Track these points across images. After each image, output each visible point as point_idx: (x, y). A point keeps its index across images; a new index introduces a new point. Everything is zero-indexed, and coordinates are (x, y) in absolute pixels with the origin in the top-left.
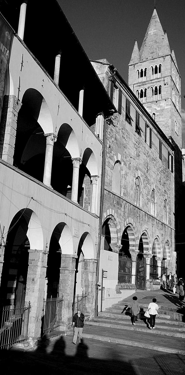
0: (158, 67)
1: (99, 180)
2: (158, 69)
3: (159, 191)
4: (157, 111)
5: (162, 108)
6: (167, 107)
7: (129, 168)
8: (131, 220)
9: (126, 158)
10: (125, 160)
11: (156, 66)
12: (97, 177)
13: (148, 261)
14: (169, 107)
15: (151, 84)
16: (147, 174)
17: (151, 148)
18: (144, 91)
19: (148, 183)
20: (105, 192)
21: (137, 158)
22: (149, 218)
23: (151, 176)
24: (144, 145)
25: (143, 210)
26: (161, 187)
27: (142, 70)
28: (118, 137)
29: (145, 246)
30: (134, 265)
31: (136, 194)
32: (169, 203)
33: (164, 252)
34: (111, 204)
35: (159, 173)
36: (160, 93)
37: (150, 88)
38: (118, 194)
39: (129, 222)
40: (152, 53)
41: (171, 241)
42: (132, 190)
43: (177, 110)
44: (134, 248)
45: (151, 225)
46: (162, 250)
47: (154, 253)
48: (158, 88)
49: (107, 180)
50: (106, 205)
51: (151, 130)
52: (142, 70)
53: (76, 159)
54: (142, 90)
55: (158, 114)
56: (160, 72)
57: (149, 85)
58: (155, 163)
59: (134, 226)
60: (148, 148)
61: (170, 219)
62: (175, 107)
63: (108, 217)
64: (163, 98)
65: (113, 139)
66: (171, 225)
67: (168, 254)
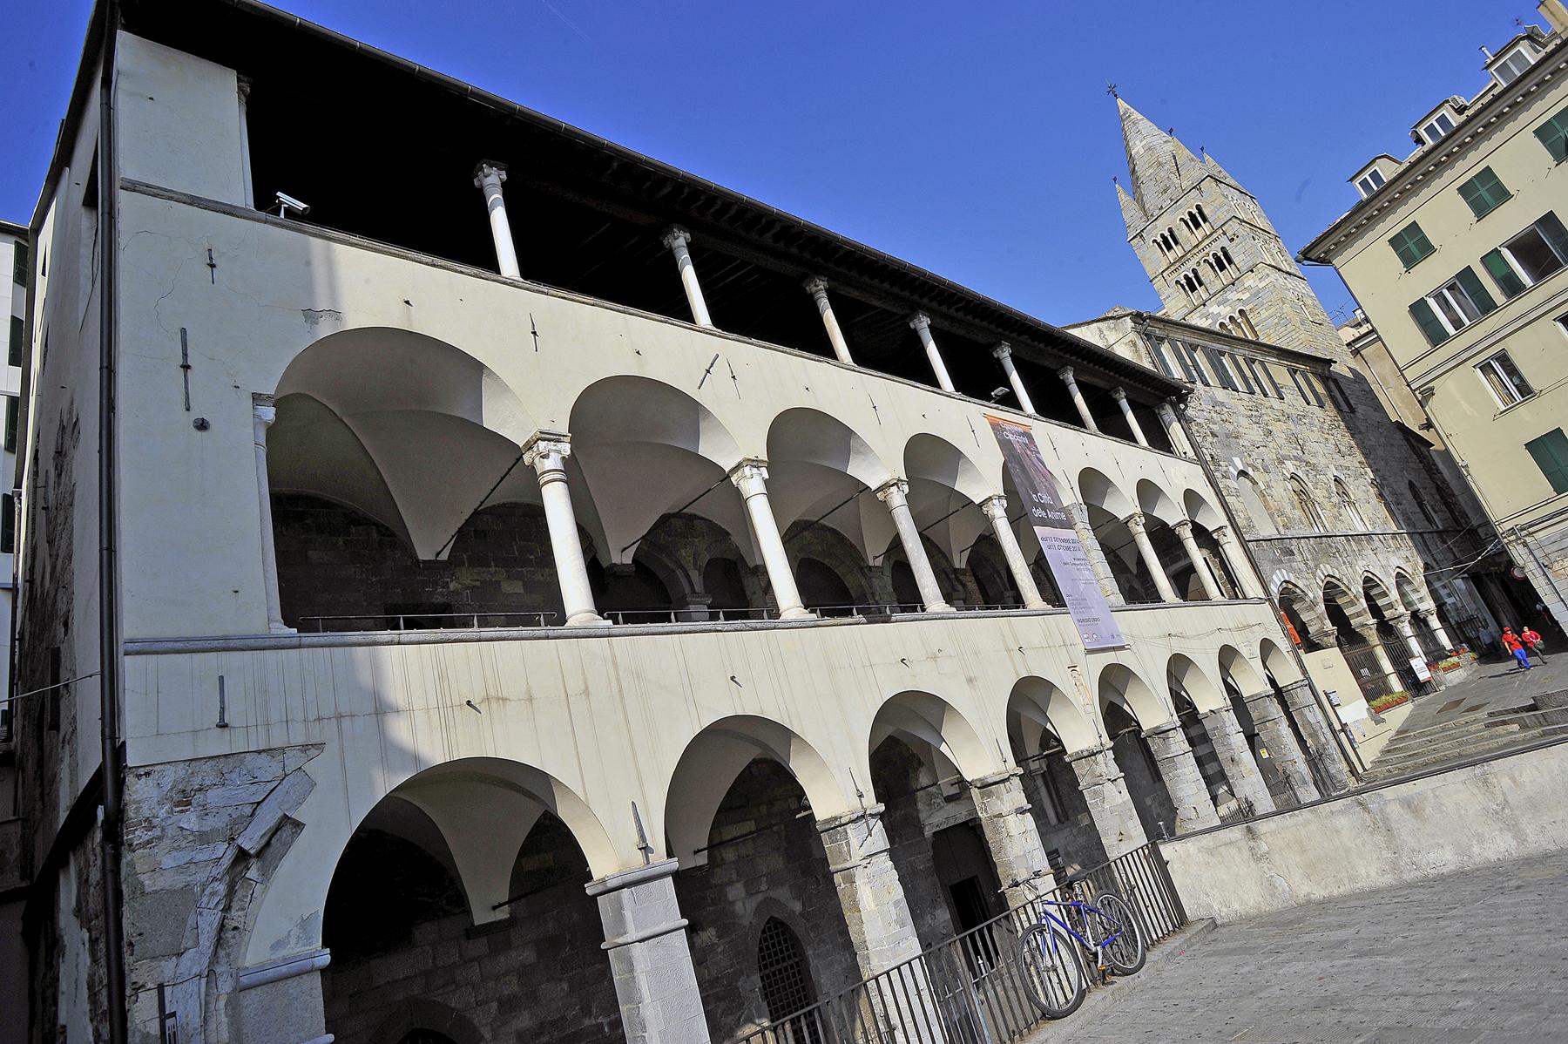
0: (1195, 211)
1: (1229, 531)
2: (1197, 215)
3: (1349, 472)
4: (1245, 302)
5: (1253, 291)
6: (1263, 284)
7: (1267, 471)
8: (1326, 569)
9: (1250, 456)
10: (1250, 461)
11: (1190, 214)
12: (1224, 530)
13: (1407, 629)
14: (1267, 281)
15: (1201, 255)
16: (1307, 457)
17: (1283, 399)
18: (1191, 275)
19: (1318, 472)
20: (1250, 545)
21: (1270, 438)
22: (1359, 543)
23: (1314, 455)
24: (1268, 405)
25: (1338, 534)
26: (1347, 461)
27: (1162, 236)
28: (1215, 428)
29: (1380, 602)
30: (1380, 652)
31: (1307, 511)
32: (1385, 482)
33: (1434, 593)
34: (1273, 561)
35: (1326, 436)
36: (1230, 262)
37: (1202, 262)
38: (1272, 533)
39: (1323, 574)
40: (1165, 191)
41: (1435, 560)
42: (1294, 508)
43: (1288, 273)
44: (1360, 619)
45: (1371, 552)
46: (1424, 591)
47: (1408, 605)
48: (1220, 254)
49: (1241, 522)
50: (1265, 568)
51: (1262, 363)
52: (1162, 236)
53: (1180, 524)
54: (1186, 277)
55: (1251, 306)
56: (1205, 220)
57: (1197, 259)
58: (1307, 421)
59: (1337, 576)
60: (1276, 403)
61: (1407, 514)
62: (1279, 270)
63: (1281, 589)
64: (1244, 269)
65: (1210, 439)
66: (1414, 526)
67: (1443, 592)
